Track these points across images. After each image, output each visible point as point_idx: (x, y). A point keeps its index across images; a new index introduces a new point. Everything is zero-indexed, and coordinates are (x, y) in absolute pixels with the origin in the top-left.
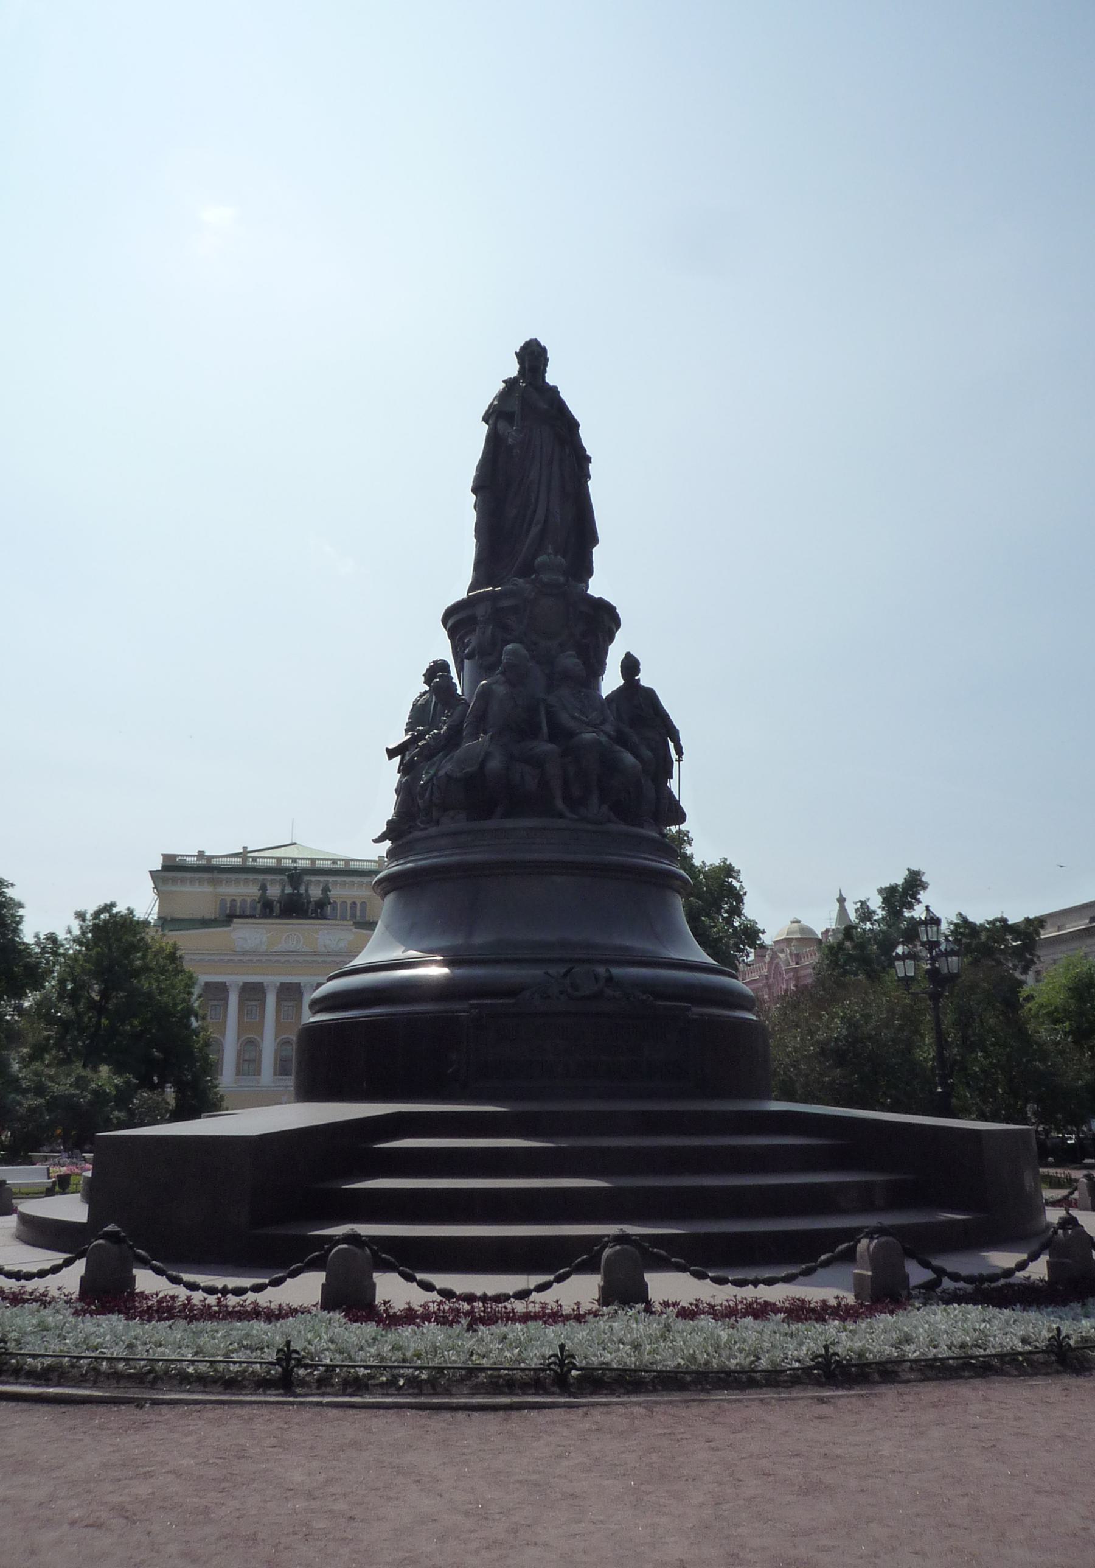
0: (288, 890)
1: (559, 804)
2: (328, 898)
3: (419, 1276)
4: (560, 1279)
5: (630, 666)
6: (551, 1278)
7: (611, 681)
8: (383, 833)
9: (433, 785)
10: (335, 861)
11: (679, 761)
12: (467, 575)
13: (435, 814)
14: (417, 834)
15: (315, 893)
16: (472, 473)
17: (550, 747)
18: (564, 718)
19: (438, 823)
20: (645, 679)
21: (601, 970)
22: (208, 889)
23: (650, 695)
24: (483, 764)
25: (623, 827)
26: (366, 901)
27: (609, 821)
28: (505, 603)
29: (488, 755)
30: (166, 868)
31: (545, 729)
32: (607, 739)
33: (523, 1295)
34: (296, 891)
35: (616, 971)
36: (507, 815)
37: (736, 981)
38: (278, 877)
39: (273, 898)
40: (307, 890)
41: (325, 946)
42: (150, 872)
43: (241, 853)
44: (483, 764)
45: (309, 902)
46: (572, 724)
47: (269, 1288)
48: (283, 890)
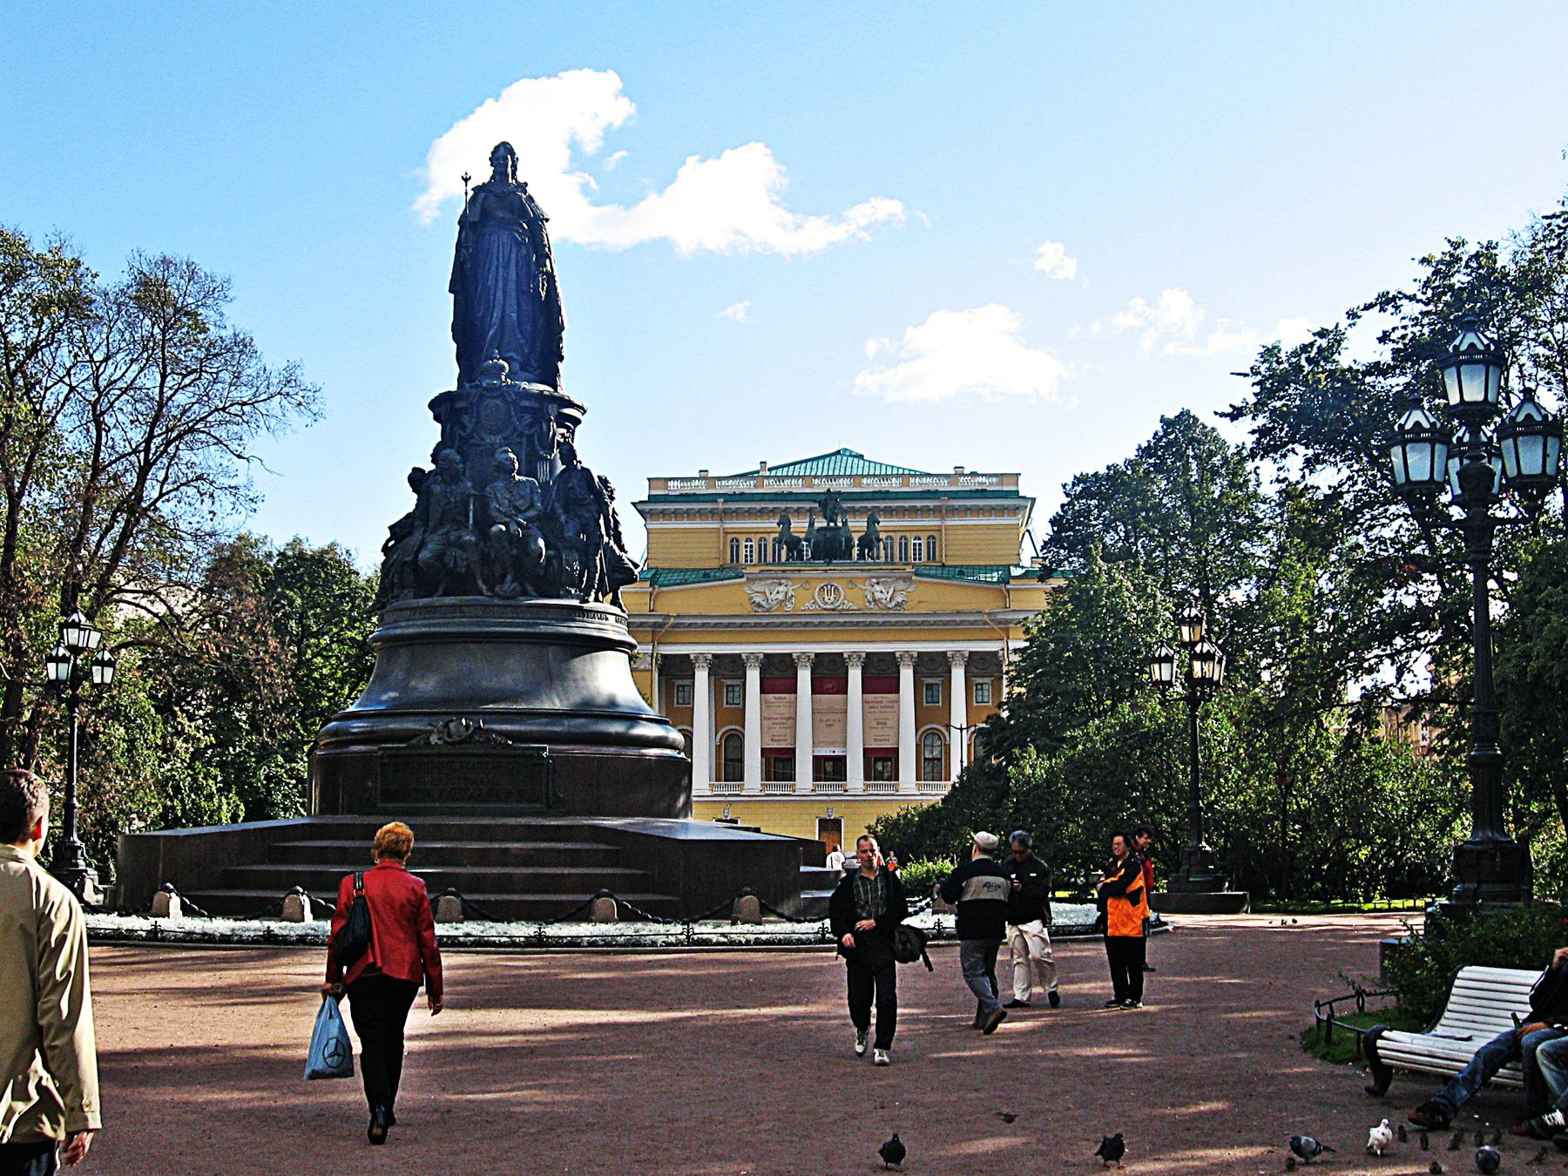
0: (821, 523)
1: (480, 582)
2: (877, 532)
10: (887, 477)
15: (858, 525)
18: (495, 505)
26: (936, 534)
27: (525, 593)
30: (652, 499)
34: (832, 524)
36: (445, 594)
38: (808, 506)
39: (802, 536)
40: (845, 523)
41: (874, 600)
42: (634, 504)
43: (757, 472)
45: (849, 540)
46: (495, 514)
48: (811, 524)
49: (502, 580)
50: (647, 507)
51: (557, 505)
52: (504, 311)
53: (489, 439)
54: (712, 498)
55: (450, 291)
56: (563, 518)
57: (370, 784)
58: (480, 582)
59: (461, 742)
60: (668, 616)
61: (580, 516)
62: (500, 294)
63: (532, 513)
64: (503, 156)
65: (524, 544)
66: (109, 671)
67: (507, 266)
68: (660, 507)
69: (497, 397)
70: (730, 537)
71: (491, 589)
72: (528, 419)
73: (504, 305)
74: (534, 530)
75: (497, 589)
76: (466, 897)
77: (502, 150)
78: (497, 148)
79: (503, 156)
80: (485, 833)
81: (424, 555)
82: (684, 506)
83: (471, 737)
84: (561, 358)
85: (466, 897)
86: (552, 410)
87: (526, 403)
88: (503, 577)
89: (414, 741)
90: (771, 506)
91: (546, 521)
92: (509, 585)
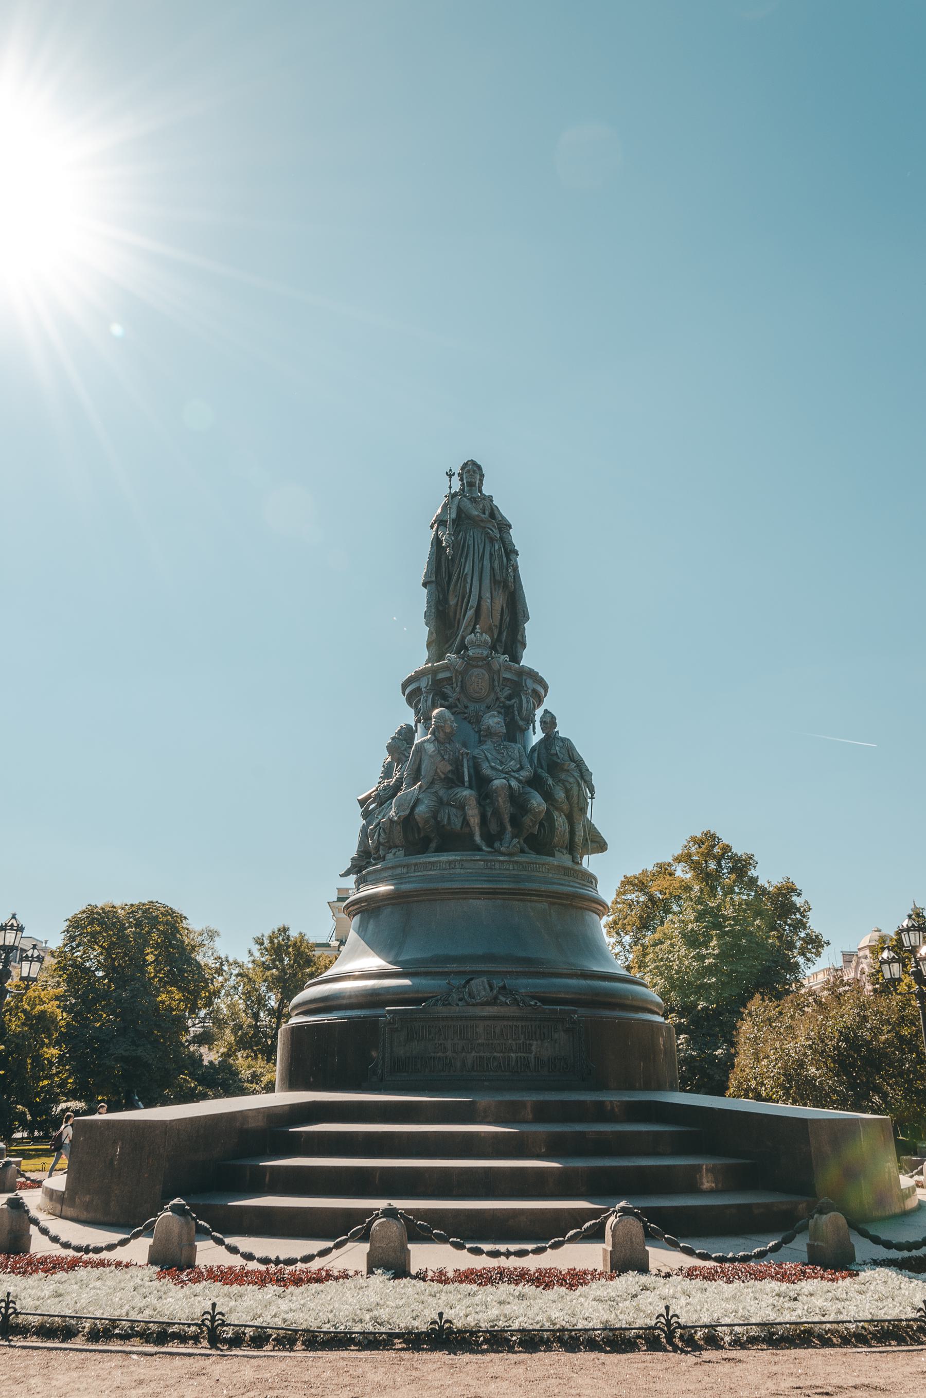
3: (228, 1241)
4: (338, 1246)
5: (549, 722)
6: (331, 1244)
7: (536, 737)
8: (349, 869)
9: (380, 828)
11: (592, 798)
13: (381, 852)
19: (384, 859)
20: (562, 730)
23: (567, 744)
24: (413, 808)
27: (522, 851)
28: (441, 676)
29: (417, 802)
31: (466, 779)
32: (517, 783)
33: (307, 1259)
37: (646, 989)
44: (413, 808)
47: (118, 1247)
49: (499, 836)
51: (540, 770)
52: (480, 598)
55: (425, 585)
56: (550, 781)
57: (374, 1054)
63: (524, 774)
66: (36, 966)
67: (482, 559)
69: (481, 667)
71: (490, 844)
72: (507, 692)
75: (497, 845)
78: (466, 464)
81: (421, 809)
83: (496, 998)
84: (524, 646)
87: (507, 675)
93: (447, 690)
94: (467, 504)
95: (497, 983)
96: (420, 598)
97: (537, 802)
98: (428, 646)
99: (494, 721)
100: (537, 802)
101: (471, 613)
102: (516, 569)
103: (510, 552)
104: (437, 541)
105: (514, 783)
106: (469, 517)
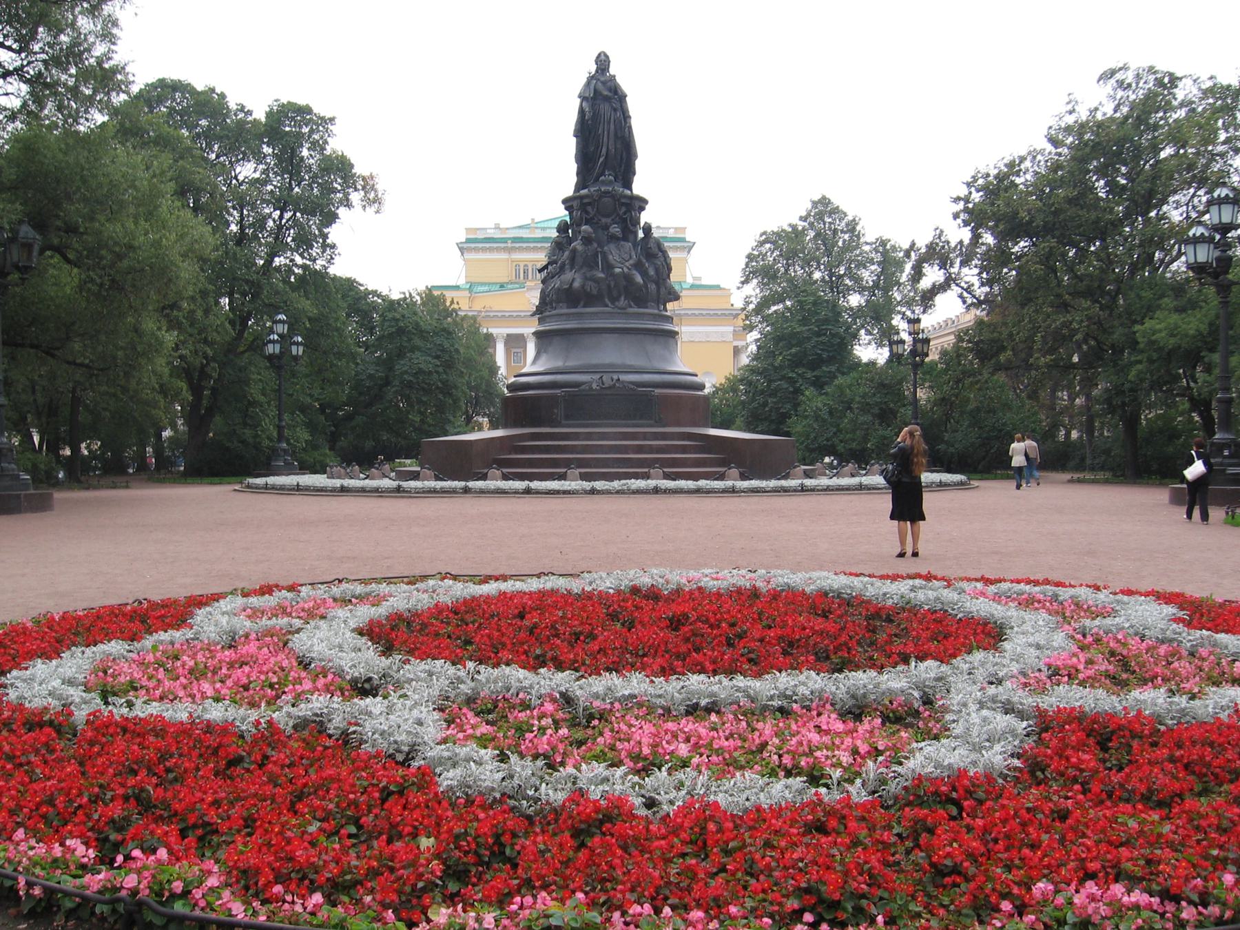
1: (606, 300)
7: (641, 234)
12: (573, 179)
14: (548, 313)
16: (572, 128)
17: (602, 275)
18: (611, 257)
21: (615, 377)
22: (504, 256)
24: (571, 284)
25: (636, 310)
27: (631, 307)
28: (585, 201)
29: (573, 280)
30: (468, 241)
35: (623, 377)
36: (585, 306)
46: (613, 262)
49: (617, 299)
50: (465, 246)
53: (604, 220)
54: (504, 240)
57: (556, 411)
58: (606, 300)
59: (610, 388)
60: (480, 311)
61: (655, 264)
62: (605, 139)
63: (631, 262)
64: (603, 62)
65: (628, 278)
67: (609, 123)
68: (473, 245)
70: (514, 264)
71: (613, 303)
72: (624, 209)
73: (608, 145)
74: (634, 272)
75: (617, 303)
76: (665, 470)
77: (603, 57)
78: (600, 55)
79: (603, 62)
80: (656, 436)
82: (487, 245)
85: (665, 470)
86: (637, 204)
87: (623, 201)
88: (620, 296)
89: (583, 387)
90: (539, 245)
91: (638, 266)
92: (622, 302)
93: (589, 209)
94: (600, 86)
95: (615, 377)
96: (570, 145)
97: (639, 279)
98: (578, 174)
99: (615, 229)
100: (639, 279)
101: (601, 160)
102: (630, 127)
103: (626, 117)
104: (582, 112)
105: (626, 270)
106: (601, 94)
